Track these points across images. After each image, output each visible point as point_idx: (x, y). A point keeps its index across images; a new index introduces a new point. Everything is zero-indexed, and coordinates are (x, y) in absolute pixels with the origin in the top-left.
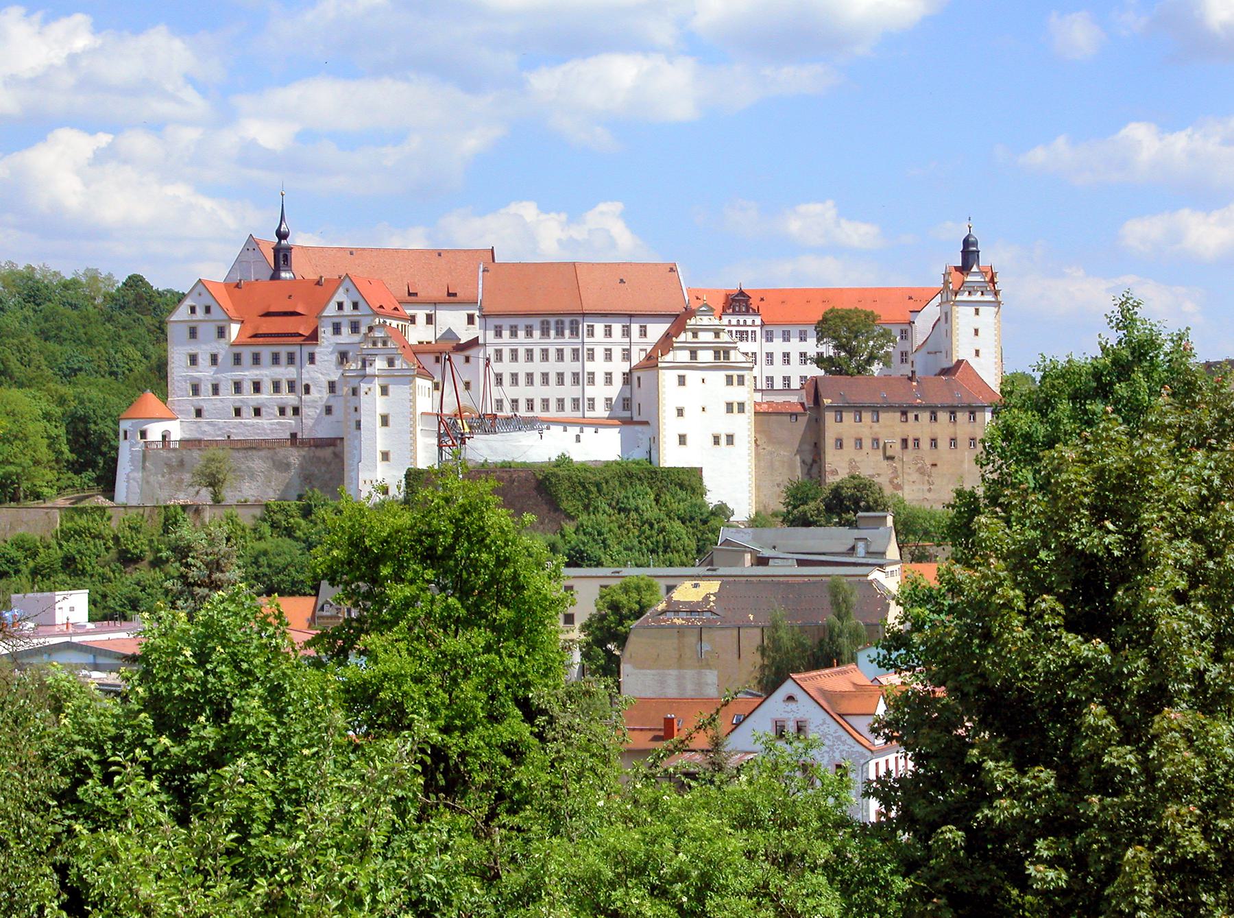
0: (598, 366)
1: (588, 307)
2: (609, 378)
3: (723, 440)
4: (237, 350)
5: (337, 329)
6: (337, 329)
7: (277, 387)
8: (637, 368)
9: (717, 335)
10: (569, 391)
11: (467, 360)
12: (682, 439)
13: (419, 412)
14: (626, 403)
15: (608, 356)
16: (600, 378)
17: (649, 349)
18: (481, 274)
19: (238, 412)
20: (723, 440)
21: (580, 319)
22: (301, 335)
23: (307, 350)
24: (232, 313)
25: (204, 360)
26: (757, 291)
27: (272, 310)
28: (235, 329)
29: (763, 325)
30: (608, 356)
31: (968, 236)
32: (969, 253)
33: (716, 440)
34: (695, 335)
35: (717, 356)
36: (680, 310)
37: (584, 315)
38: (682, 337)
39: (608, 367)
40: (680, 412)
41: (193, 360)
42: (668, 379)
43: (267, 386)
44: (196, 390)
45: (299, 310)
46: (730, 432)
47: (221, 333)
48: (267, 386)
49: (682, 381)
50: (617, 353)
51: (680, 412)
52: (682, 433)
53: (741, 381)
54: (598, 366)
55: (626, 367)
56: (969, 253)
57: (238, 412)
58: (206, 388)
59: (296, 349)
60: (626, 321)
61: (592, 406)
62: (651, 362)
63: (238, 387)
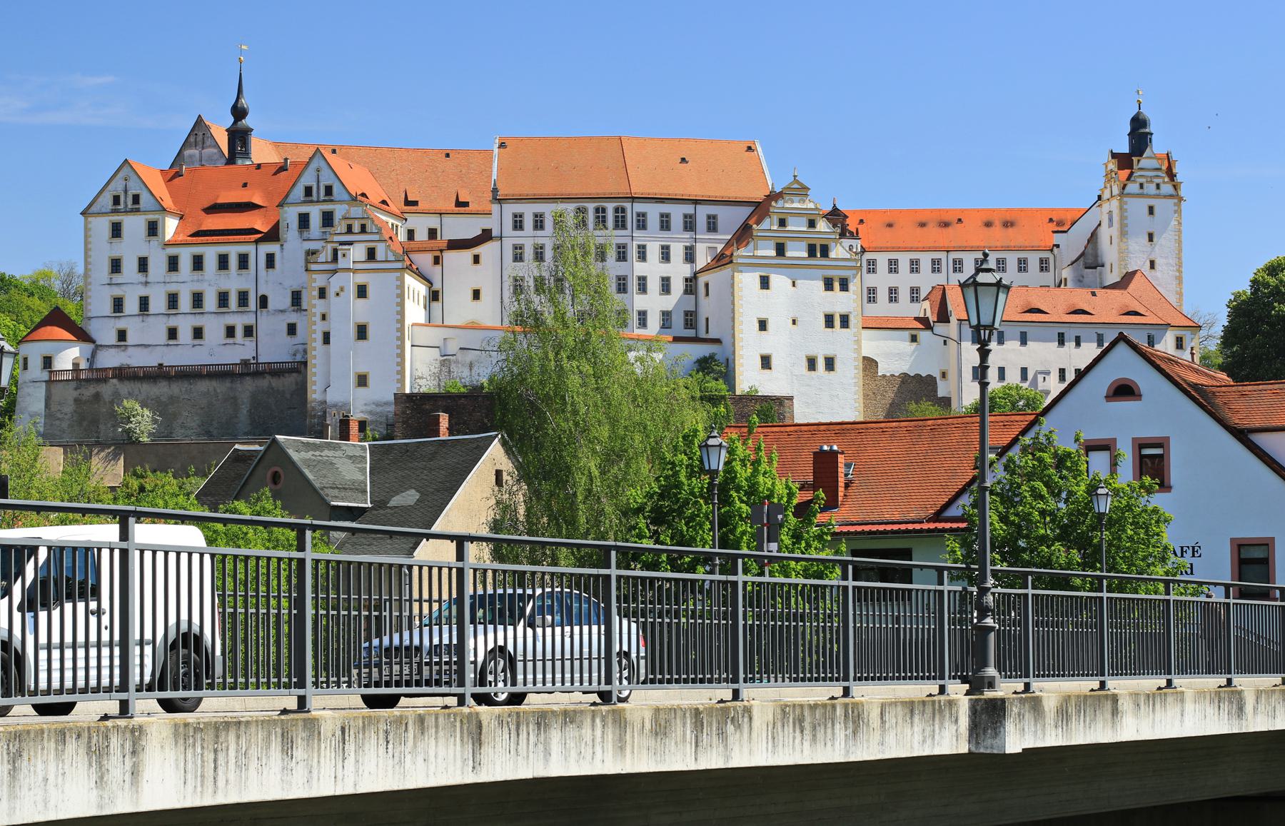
0: (652, 269)
1: (637, 190)
2: (666, 285)
3: (821, 364)
4: (173, 251)
5: (304, 221)
6: (304, 221)
7: (223, 299)
8: (702, 271)
9: (812, 224)
11: (476, 259)
12: (766, 362)
13: (408, 322)
14: (691, 319)
15: (666, 255)
16: (654, 285)
17: (720, 247)
18: (496, 151)
19: (173, 333)
20: (821, 364)
21: (628, 205)
22: (257, 232)
23: (266, 248)
24: (168, 202)
25: (130, 266)
26: (855, 212)
27: (220, 201)
28: (171, 226)
29: (864, 251)
30: (666, 255)
31: (1138, 113)
32: (1139, 133)
33: (812, 364)
34: (782, 223)
35: (812, 251)
36: (759, 195)
37: (633, 199)
38: (766, 224)
39: (665, 269)
40: (763, 325)
41: (116, 266)
42: (747, 281)
43: (210, 302)
44: (118, 304)
45: (257, 200)
46: (830, 353)
47: (153, 229)
48: (210, 302)
49: (765, 283)
50: (677, 251)
51: (763, 325)
52: (765, 352)
53: (844, 286)
54: (652, 269)
55: (687, 270)
56: (1139, 133)
57: (173, 333)
58: (131, 306)
59: (249, 249)
60: (689, 209)
61: (643, 322)
62: (722, 260)
63: (173, 300)
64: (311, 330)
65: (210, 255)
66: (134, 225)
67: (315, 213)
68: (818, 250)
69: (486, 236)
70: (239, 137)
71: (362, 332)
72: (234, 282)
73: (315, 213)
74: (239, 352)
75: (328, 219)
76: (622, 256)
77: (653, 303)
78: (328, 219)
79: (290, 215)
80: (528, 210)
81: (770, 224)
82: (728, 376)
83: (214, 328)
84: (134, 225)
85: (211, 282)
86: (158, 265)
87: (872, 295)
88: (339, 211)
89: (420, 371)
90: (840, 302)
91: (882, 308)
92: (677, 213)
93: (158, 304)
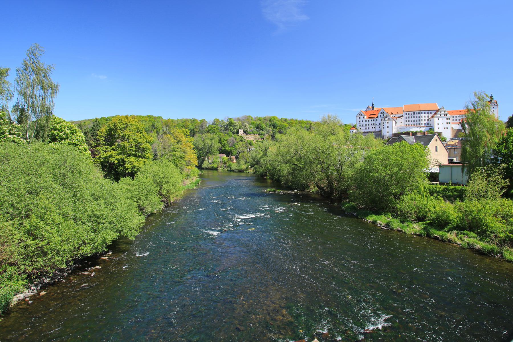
0: (423, 118)
2: (425, 120)
5: (381, 116)
6: (381, 116)
10: (418, 122)
12: (439, 128)
14: (428, 124)
15: (425, 117)
16: (423, 120)
25: (361, 121)
28: (366, 117)
30: (425, 117)
42: (436, 119)
50: (426, 116)
54: (423, 118)
58: (361, 126)
62: (432, 117)
64: (382, 127)
65: (370, 120)
66: (362, 117)
67: (382, 115)
68: (446, 115)
69: (401, 116)
70: (373, 108)
71: (388, 127)
72: (373, 122)
73: (382, 115)
74: (374, 130)
75: (383, 115)
76: (419, 117)
77: (423, 122)
78: (383, 115)
79: (379, 115)
80: (407, 113)
81: (439, 112)
82: (434, 130)
83: (371, 127)
84: (362, 117)
85: (370, 123)
86: (364, 121)
87: (453, 120)
88: (385, 114)
89: (395, 131)
90: (448, 121)
91: (455, 122)
92: (426, 112)
93: (364, 125)
